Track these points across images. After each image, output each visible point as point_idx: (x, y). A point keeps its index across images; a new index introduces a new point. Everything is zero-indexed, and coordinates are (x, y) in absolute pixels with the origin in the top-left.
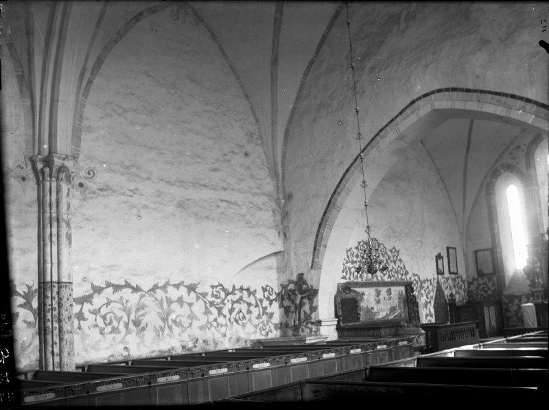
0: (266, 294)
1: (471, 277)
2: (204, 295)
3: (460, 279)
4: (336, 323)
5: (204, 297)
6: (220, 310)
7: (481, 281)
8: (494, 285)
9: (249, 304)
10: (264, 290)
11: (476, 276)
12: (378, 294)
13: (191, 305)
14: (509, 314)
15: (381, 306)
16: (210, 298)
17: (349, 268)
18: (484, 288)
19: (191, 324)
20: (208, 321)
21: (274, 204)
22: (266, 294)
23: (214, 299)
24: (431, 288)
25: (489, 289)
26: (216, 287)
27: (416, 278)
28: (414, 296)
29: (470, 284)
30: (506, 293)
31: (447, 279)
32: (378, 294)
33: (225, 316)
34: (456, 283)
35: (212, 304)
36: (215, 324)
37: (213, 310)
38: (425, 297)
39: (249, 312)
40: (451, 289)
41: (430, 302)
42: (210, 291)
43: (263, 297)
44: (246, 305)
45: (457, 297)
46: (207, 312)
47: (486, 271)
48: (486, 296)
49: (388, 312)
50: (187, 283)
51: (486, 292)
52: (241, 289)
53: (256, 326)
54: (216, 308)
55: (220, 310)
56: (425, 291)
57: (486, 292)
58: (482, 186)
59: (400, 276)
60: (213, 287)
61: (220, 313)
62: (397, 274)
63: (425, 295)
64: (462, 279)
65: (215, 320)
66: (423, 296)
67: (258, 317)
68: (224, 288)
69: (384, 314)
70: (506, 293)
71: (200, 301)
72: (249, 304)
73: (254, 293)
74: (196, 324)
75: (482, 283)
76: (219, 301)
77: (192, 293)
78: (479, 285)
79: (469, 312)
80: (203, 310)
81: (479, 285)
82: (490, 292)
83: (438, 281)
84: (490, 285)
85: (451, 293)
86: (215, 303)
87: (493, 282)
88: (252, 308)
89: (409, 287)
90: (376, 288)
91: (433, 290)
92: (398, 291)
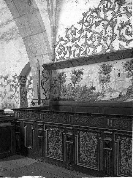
2: (10, 81)
5: (10, 82)
6: (16, 88)
12: (107, 70)
13: (5, 86)
15: (111, 84)
16: (12, 83)
19: (5, 96)
20: (11, 95)
23: (14, 83)
26: (14, 76)
32: (107, 70)
33: (18, 93)
35: (13, 85)
36: (14, 96)
37: (14, 89)
42: (12, 79)
46: (11, 90)
49: (124, 93)
50: (4, 76)
54: (15, 88)
55: (16, 88)
60: (13, 76)
61: (16, 91)
65: (14, 94)
68: (17, 76)
69: (116, 95)
71: (9, 84)
74: (7, 96)
76: (16, 84)
77: (6, 80)
80: (9, 89)
86: (15, 85)
90: (102, 64)
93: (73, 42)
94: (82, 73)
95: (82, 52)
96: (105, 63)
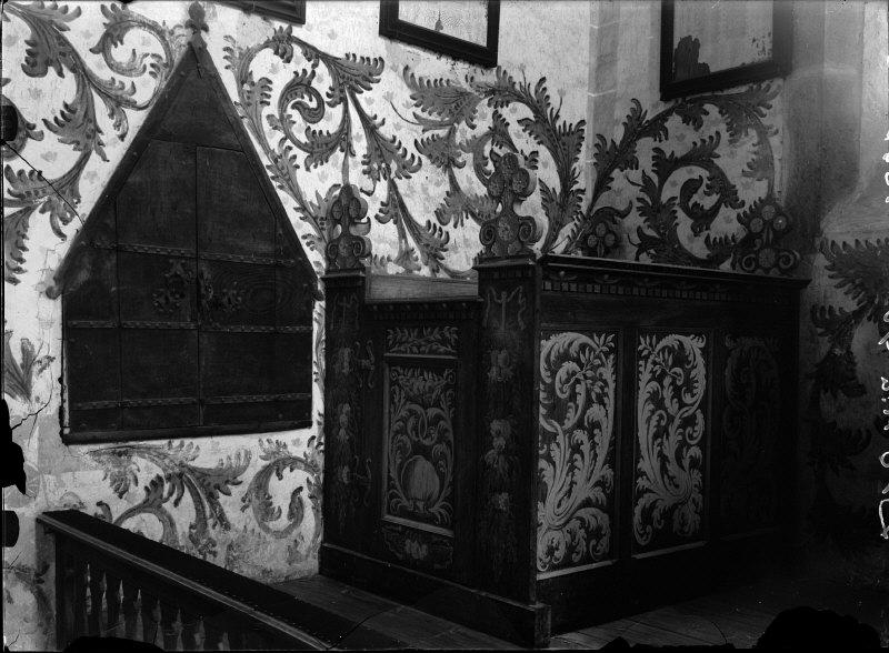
1: (622, 112)
3: (516, 113)
7: (680, 137)
8: (760, 167)
11: (652, 106)
18: (690, 187)
25: (728, 195)
29: (613, 158)
31: (353, 77)
34: (463, 133)
47: (716, 57)
48: (698, 249)
51: (702, 219)
57: (702, 219)
70: (839, 228)
79: (436, 367)
81: (665, 165)
82: (727, 224)
84: (734, 160)
91: (76, 125)
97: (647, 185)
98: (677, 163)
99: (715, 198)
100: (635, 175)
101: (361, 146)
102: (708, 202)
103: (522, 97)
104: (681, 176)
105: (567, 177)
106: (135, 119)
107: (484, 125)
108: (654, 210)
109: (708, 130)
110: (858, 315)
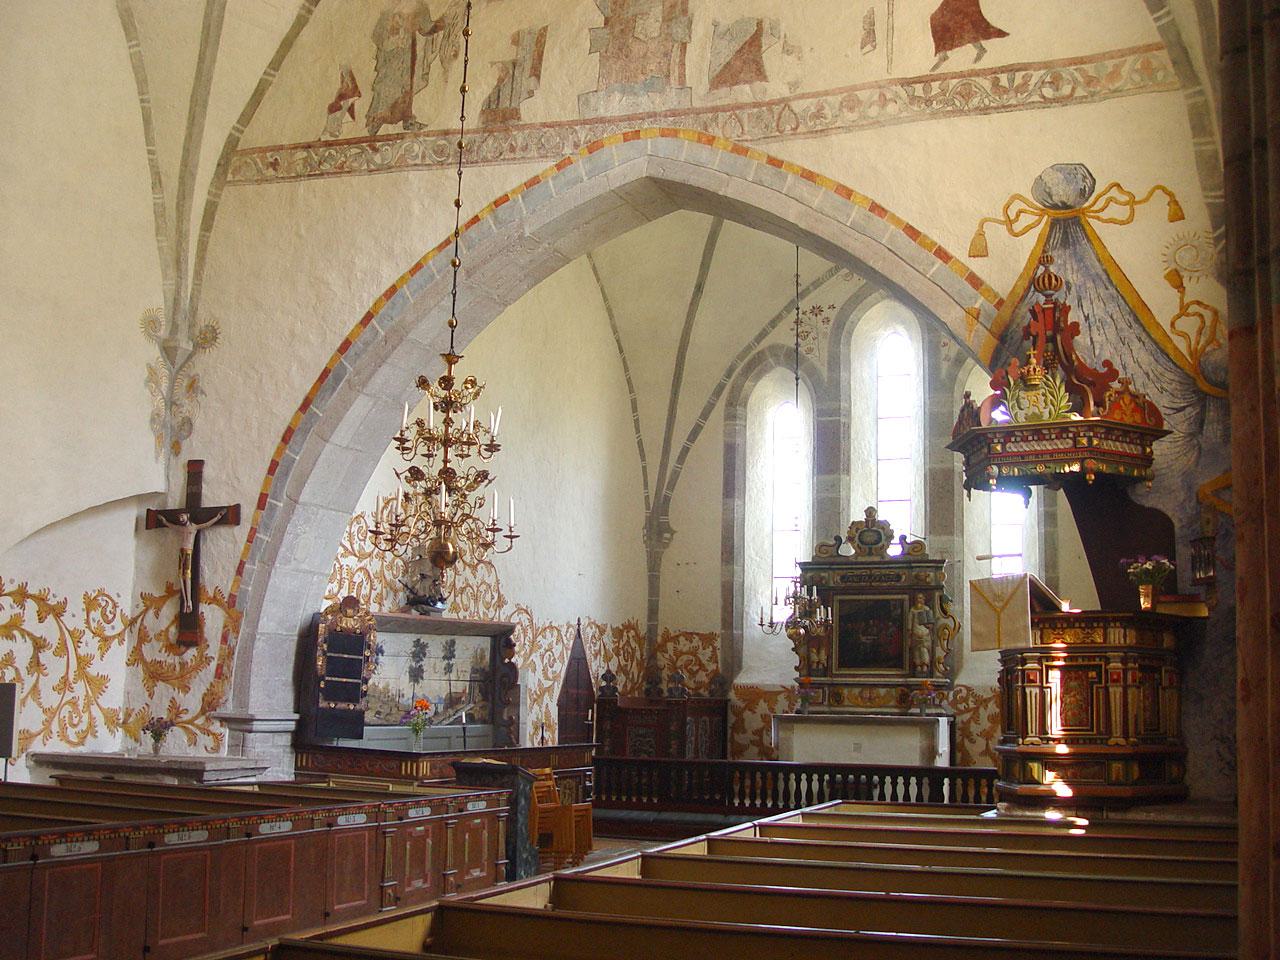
0: (96, 615)
4: (292, 726)
8: (713, 658)
9: (39, 645)
10: (90, 603)
12: (420, 652)
14: (740, 738)
17: (349, 569)
21: (154, 353)
22: (96, 615)
24: (558, 649)
25: (702, 666)
27: (524, 617)
28: (513, 666)
30: (741, 680)
38: (539, 674)
39: (36, 665)
40: (607, 659)
41: (550, 689)
43: (82, 626)
44: (29, 643)
45: (621, 682)
51: (693, 674)
52: (21, 595)
53: (51, 713)
56: (542, 656)
57: (693, 674)
58: (718, 392)
59: (482, 609)
62: (476, 600)
63: (539, 668)
64: (637, 635)
66: (534, 670)
67: (65, 685)
72: (39, 645)
73: (51, 610)
75: (684, 650)
78: (679, 654)
81: (679, 654)
82: (702, 677)
83: (579, 631)
84: (705, 655)
85: (609, 671)
87: (714, 648)
88: (46, 657)
89: (501, 638)
92: (471, 650)
93: (360, 560)
94: (382, 652)
95: (374, 593)
96: (419, 636)
97: (671, 660)
98: (682, 653)
99: (698, 667)
100: (667, 656)
101: (602, 653)
102: (695, 668)
103: (633, 629)
104: (685, 658)
105: (642, 655)
106: (569, 652)
107: (625, 638)
108: (674, 667)
109: (695, 644)
110: (745, 709)
